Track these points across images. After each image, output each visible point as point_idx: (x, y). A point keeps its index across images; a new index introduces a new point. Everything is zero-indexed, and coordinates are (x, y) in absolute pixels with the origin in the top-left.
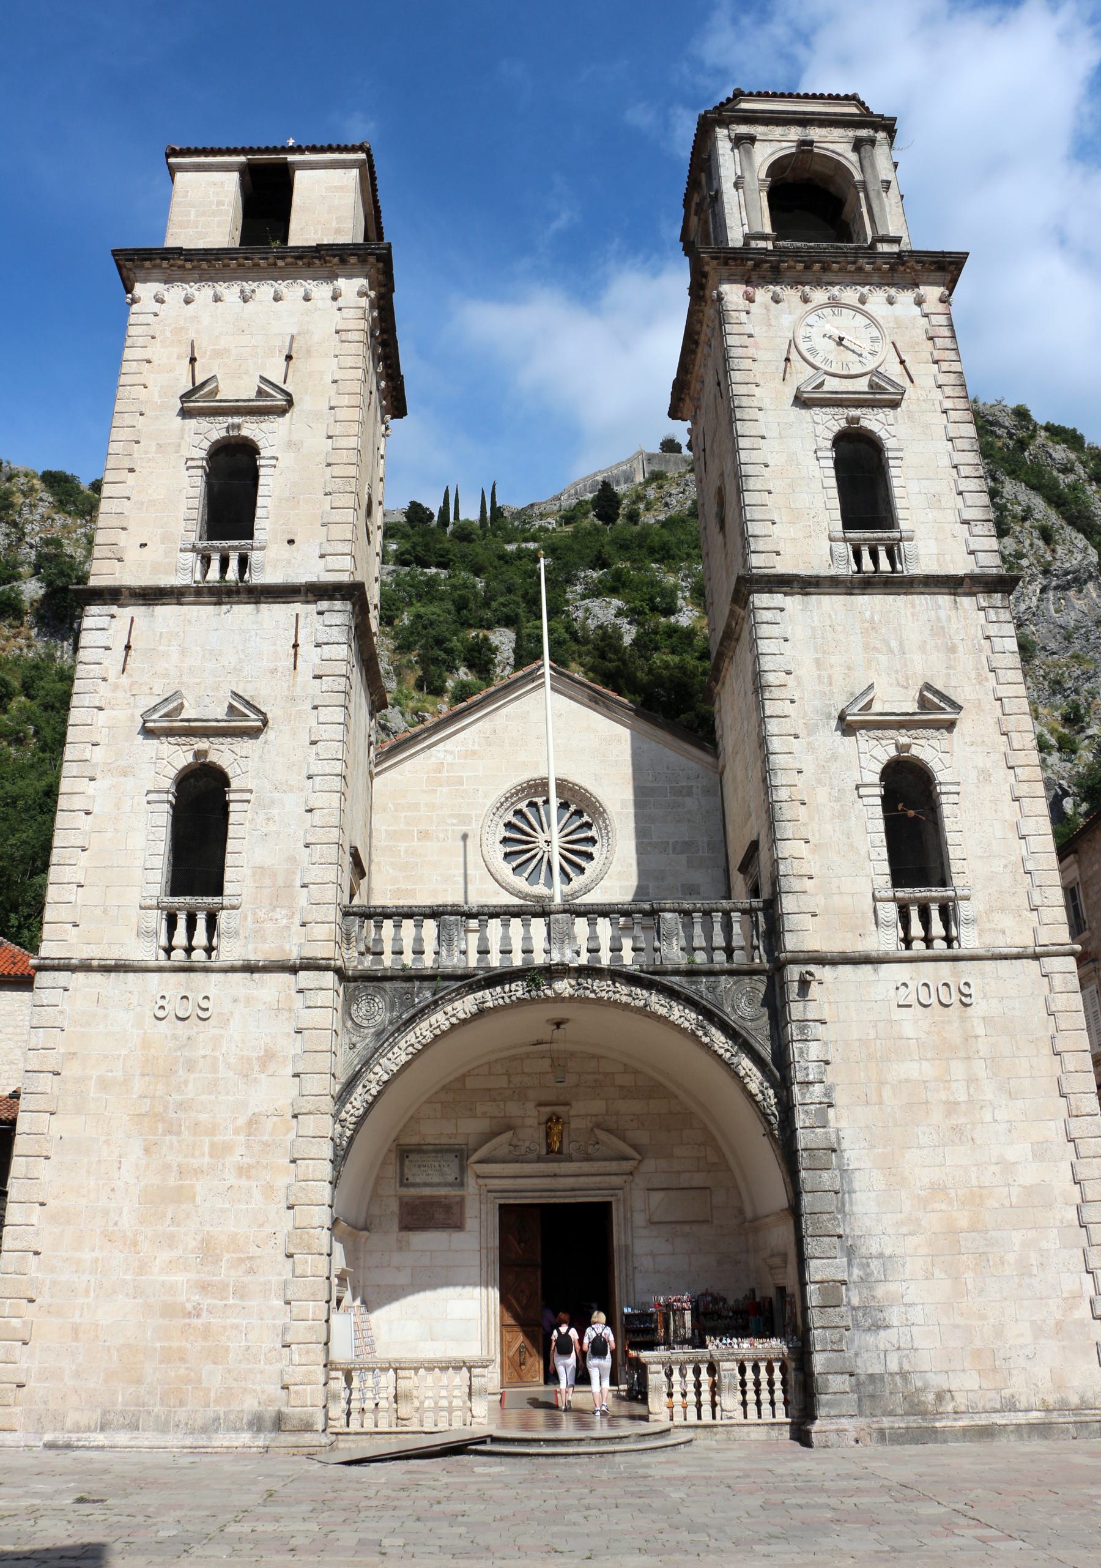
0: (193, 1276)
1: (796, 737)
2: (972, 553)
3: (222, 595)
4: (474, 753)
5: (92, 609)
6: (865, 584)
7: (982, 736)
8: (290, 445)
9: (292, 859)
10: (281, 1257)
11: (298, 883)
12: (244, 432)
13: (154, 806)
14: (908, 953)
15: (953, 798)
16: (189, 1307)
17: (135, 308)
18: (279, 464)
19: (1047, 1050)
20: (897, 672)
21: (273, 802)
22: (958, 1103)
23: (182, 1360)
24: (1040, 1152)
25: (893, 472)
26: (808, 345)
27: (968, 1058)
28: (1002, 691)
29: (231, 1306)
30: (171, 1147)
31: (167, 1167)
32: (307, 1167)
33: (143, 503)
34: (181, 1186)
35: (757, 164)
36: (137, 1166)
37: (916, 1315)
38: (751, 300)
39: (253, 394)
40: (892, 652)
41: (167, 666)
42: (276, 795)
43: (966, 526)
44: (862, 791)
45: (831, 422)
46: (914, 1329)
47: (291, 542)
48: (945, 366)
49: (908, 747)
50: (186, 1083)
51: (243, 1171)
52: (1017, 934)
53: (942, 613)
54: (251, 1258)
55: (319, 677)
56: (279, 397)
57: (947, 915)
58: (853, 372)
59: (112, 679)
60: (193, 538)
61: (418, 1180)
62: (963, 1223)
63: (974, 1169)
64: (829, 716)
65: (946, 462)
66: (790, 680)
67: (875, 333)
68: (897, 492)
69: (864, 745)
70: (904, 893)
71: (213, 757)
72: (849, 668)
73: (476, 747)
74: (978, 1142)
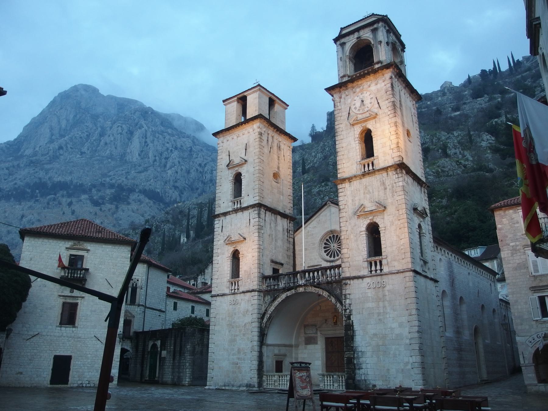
3: (236, 211)
5: (216, 219)
6: (364, 175)
8: (247, 171)
9: (250, 268)
12: (239, 171)
15: (384, 231)
19: (403, 298)
24: (401, 325)
28: (398, 198)
37: (369, 366)
44: (361, 233)
48: (389, 100)
49: (372, 219)
52: (398, 266)
53: (384, 179)
60: (232, 199)
61: (308, 332)
62: (381, 344)
70: (370, 259)
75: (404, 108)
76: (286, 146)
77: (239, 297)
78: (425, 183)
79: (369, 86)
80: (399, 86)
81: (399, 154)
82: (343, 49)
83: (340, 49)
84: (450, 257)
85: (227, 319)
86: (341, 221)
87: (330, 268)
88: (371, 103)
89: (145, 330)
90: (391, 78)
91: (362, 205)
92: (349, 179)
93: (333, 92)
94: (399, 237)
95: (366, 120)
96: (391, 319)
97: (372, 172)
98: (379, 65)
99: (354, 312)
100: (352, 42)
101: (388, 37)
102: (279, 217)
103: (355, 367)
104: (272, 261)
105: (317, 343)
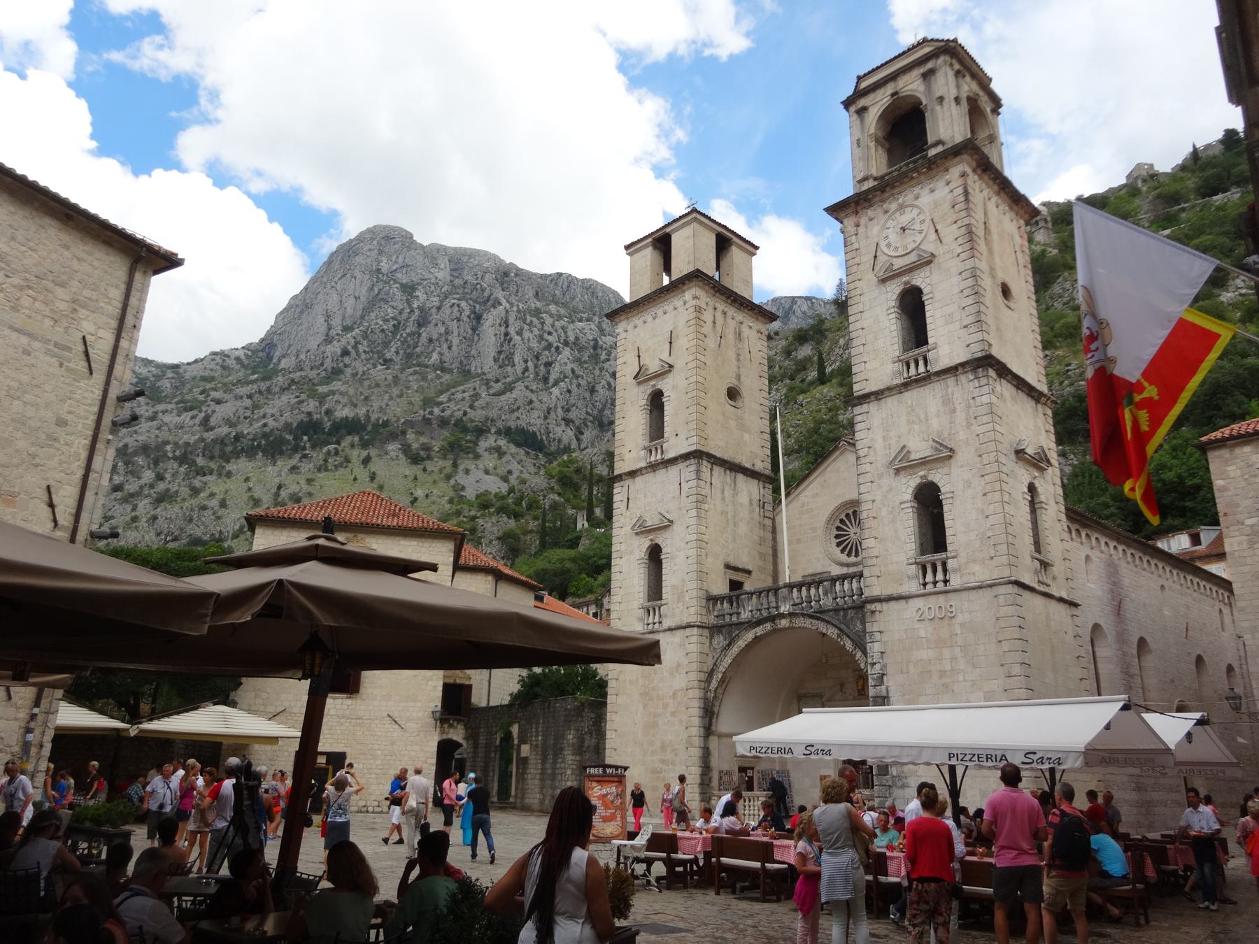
3: (653, 467)
8: (674, 387)
9: (683, 580)
25: (927, 308)
28: (980, 430)
45: (895, 289)
51: (673, 714)
52: (981, 573)
53: (950, 390)
60: (646, 443)
65: (957, 290)
66: (872, 453)
69: (904, 480)
75: (995, 237)
76: (753, 331)
78: (1045, 396)
79: (917, 198)
80: (981, 192)
81: (979, 336)
82: (862, 120)
83: (858, 122)
84: (1112, 551)
86: (861, 481)
87: (843, 578)
89: (492, 704)
90: (963, 175)
91: (904, 447)
92: (877, 395)
93: (842, 215)
94: (982, 511)
95: (911, 269)
97: (924, 379)
98: (940, 149)
99: (890, 670)
101: (958, 87)
102: (740, 477)
103: (894, 782)
104: (728, 567)
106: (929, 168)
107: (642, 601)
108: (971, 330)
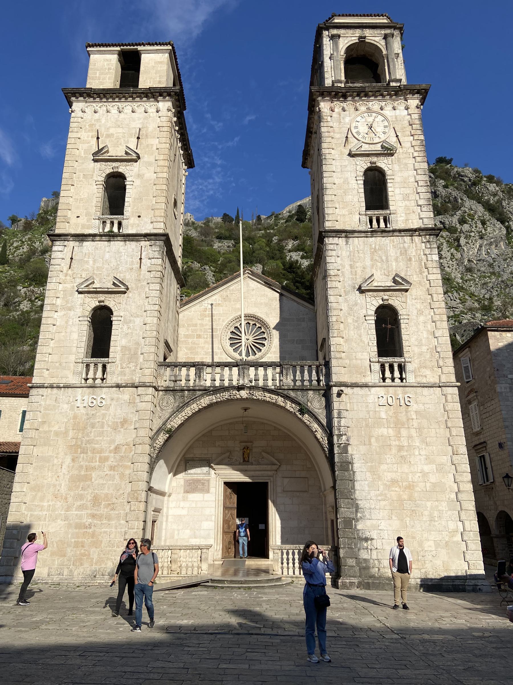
0: (89, 512)
1: (341, 296)
2: (421, 219)
3: (111, 236)
4: (219, 304)
5: (58, 243)
6: (373, 233)
7: (420, 295)
9: (138, 344)
10: (126, 503)
11: (140, 353)
12: (120, 170)
13: (83, 323)
14: (384, 384)
15: (405, 321)
16: (87, 524)
17: (73, 115)
18: (134, 184)
19: (443, 426)
20: (384, 269)
21: (130, 321)
22: (404, 447)
23: (83, 546)
25: (389, 185)
26: (356, 130)
27: (409, 428)
28: (430, 277)
29: (104, 524)
30: (83, 458)
31: (81, 467)
32: (138, 466)
33: (78, 199)
34: (87, 474)
35: (340, 48)
36: (69, 466)
38: (333, 111)
39: (123, 154)
40: (383, 261)
41: (88, 266)
42: (132, 318)
43: (419, 207)
45: (363, 164)
46: (383, 540)
47: (139, 217)
48: (416, 137)
50: (91, 432)
51: (112, 468)
53: (406, 245)
54: (113, 504)
55: (150, 271)
56: (134, 155)
57: (402, 368)
58: (374, 142)
59: (65, 272)
60: (99, 214)
63: (411, 474)
64: (354, 287)
65: (413, 180)
67: (386, 124)
68: (390, 194)
70: (383, 359)
71: (107, 303)
72: (364, 268)
73: (220, 302)
74: (412, 463)
77: (104, 393)
79: (382, 109)
85: (71, 434)
88: (384, 133)
91: (373, 275)
96: (423, 458)
100: (350, 39)
105: (208, 491)
106: (396, 94)
107: (82, 356)
108: (423, 209)
